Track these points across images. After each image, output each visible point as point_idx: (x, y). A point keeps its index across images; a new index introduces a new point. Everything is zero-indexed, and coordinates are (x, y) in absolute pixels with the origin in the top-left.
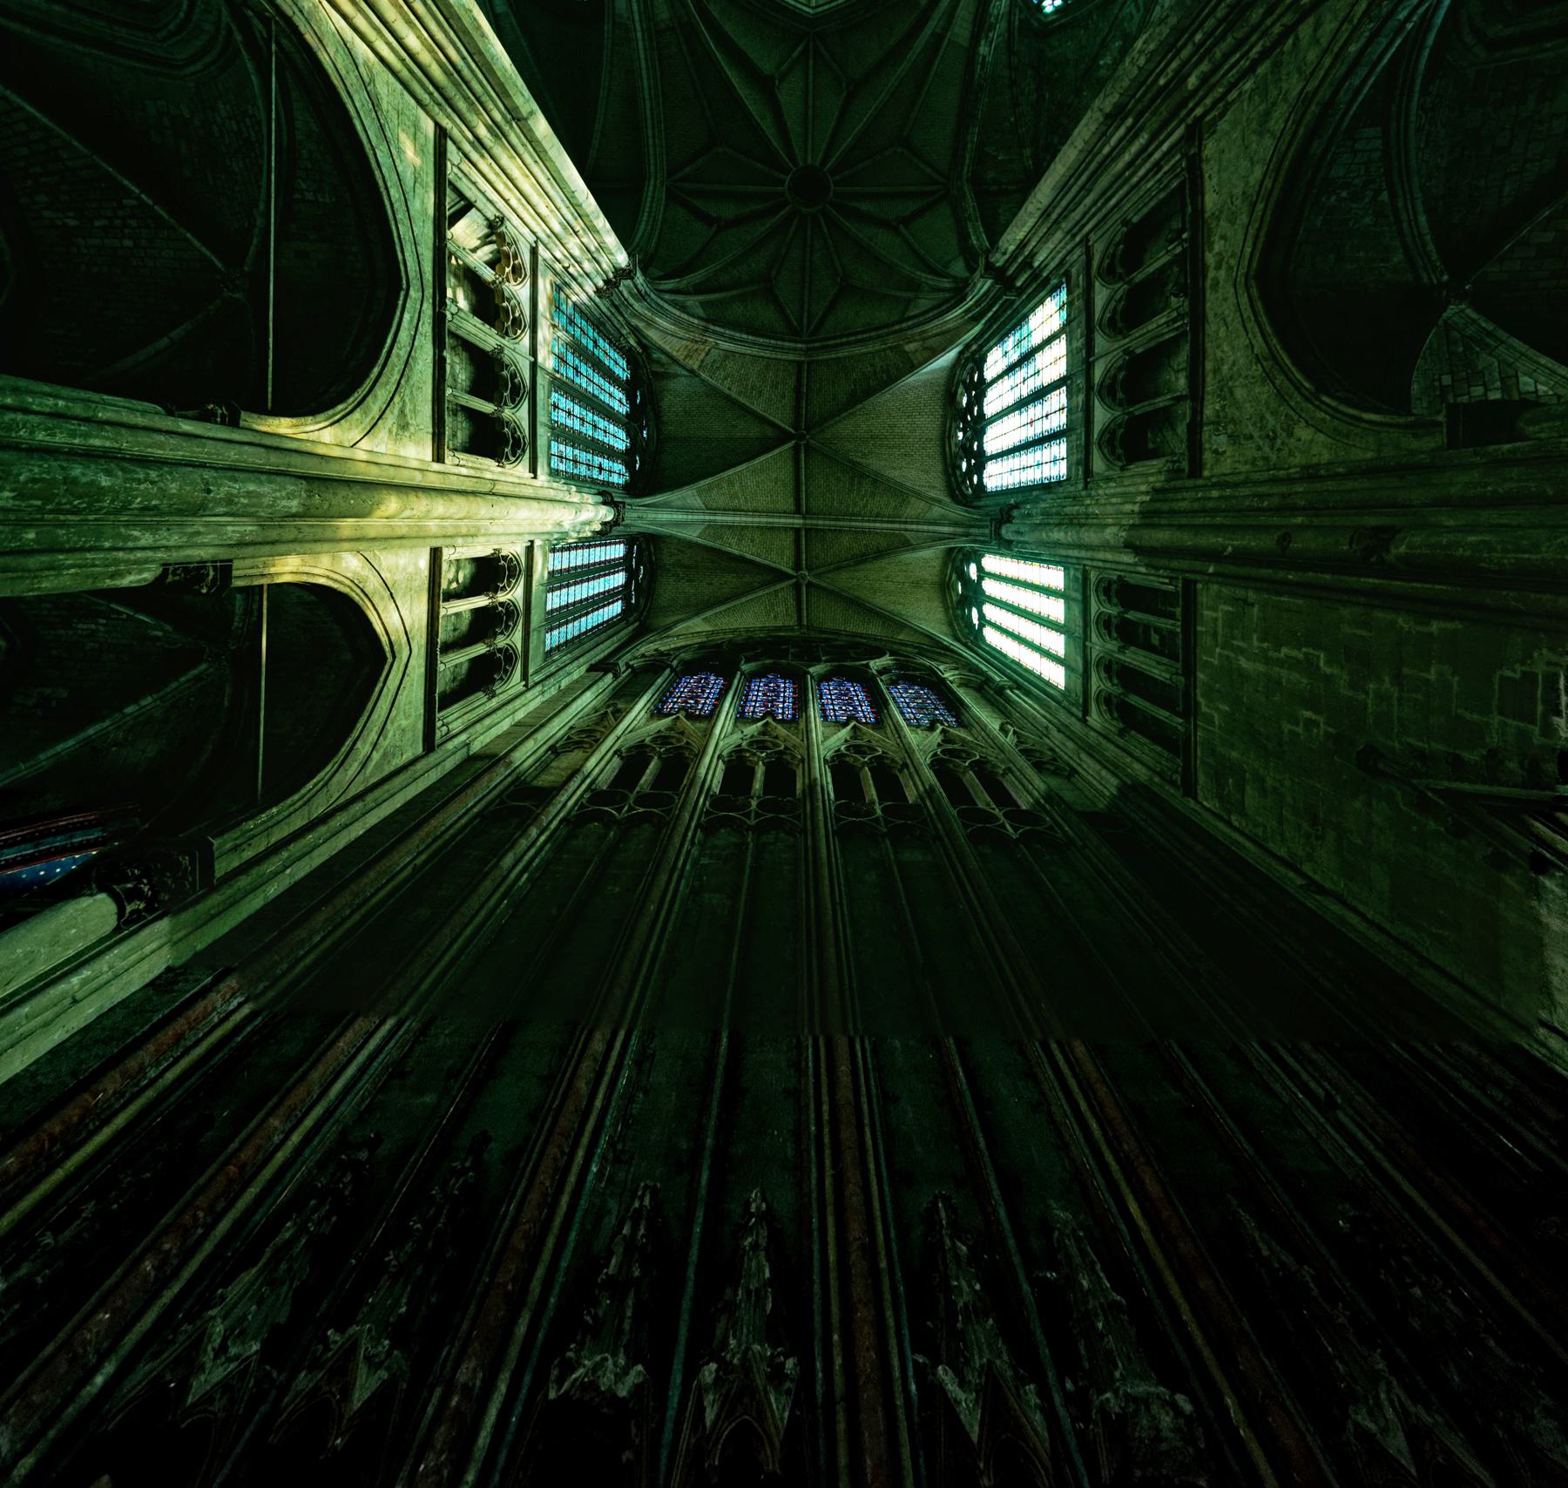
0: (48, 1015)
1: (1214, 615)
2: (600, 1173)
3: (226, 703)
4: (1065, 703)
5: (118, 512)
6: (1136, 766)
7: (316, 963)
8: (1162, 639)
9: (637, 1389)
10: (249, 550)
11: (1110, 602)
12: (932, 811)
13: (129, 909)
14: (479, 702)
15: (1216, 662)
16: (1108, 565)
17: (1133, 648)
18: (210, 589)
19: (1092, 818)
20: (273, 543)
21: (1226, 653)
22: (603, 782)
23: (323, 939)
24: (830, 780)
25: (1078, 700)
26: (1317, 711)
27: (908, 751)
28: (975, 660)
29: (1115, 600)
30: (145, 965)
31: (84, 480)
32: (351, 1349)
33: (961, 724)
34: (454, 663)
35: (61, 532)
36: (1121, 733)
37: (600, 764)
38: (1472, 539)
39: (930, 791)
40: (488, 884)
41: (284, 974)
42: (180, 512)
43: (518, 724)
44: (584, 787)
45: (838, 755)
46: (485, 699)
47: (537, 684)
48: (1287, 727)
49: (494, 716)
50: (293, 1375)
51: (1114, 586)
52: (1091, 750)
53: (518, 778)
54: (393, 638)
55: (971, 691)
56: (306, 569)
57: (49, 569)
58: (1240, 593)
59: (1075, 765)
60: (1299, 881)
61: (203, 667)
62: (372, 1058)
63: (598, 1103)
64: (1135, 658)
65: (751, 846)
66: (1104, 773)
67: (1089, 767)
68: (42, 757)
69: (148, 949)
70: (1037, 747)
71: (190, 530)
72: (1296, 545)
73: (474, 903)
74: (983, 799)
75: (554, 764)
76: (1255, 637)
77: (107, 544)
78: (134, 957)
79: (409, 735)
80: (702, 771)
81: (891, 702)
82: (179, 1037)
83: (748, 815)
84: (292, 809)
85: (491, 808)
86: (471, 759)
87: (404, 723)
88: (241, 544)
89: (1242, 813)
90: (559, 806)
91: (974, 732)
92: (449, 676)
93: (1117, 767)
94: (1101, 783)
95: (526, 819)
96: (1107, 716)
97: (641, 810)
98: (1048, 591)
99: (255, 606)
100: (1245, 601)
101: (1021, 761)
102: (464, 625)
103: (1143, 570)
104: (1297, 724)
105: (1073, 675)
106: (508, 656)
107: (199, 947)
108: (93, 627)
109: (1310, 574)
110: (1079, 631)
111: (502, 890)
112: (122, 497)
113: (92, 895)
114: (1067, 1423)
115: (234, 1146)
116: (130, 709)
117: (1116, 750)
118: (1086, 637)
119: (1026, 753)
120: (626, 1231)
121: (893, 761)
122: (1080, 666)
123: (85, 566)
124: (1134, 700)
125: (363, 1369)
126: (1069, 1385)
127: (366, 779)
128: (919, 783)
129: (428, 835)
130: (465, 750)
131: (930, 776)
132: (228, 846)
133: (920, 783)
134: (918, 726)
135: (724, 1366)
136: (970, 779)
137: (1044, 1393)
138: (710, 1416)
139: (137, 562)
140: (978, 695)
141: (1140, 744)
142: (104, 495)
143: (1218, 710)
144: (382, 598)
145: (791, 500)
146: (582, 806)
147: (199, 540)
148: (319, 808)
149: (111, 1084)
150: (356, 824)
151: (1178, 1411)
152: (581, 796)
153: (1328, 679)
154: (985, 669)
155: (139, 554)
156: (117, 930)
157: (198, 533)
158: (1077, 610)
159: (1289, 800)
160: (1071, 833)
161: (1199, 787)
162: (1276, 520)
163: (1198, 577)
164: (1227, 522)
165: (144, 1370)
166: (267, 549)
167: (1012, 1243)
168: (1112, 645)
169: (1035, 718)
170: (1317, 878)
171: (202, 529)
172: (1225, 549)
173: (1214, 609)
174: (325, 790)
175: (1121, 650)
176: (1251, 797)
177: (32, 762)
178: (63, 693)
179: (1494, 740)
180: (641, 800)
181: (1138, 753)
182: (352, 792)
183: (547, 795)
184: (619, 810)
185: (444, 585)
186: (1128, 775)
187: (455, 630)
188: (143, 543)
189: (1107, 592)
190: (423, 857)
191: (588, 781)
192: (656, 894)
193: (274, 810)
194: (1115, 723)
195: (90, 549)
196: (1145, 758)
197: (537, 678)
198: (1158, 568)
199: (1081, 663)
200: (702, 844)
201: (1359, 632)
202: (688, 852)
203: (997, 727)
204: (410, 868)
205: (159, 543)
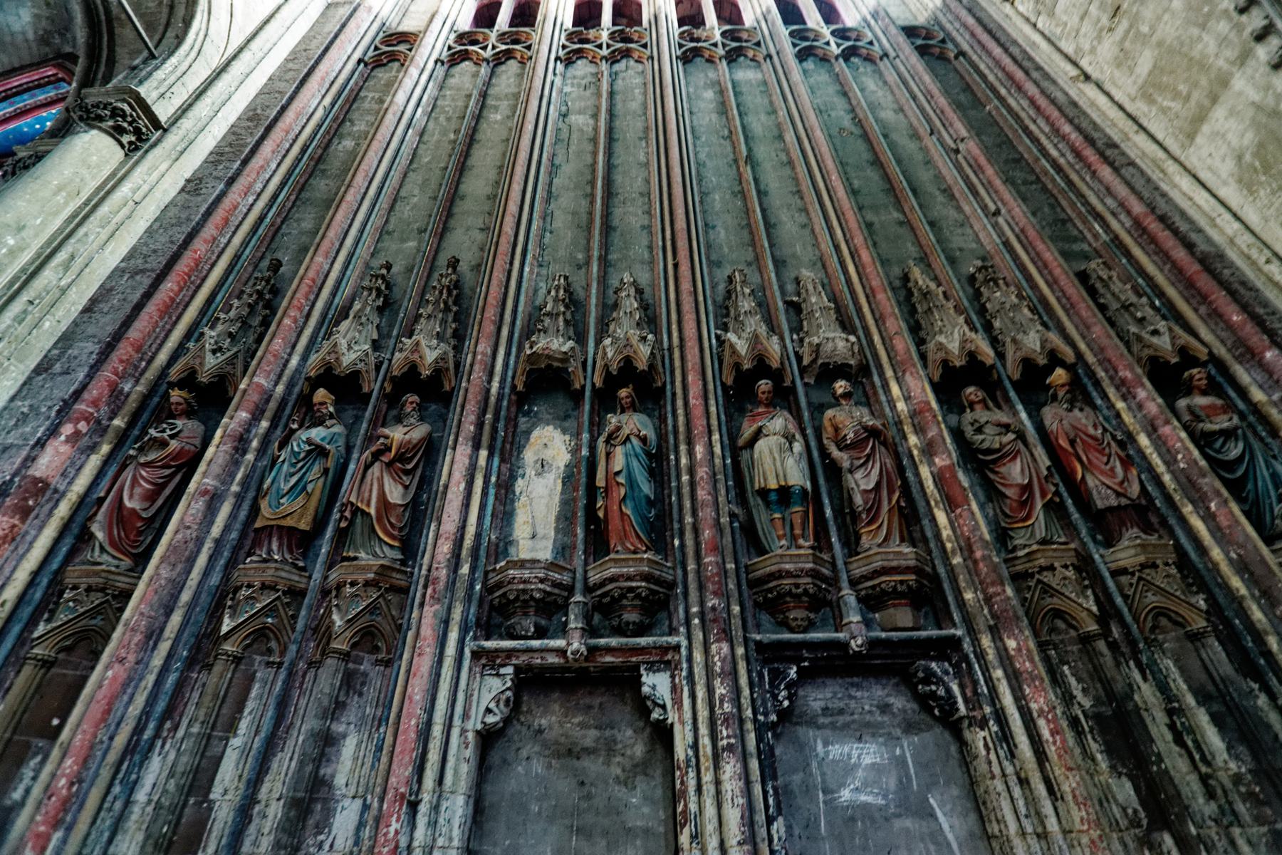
2: (531, 272)
9: (572, 349)
23: (279, 165)
32: (418, 344)
40: (390, 119)
60: (1074, 72)
62: (364, 225)
73: (384, 132)
83: (600, 46)
89: (1051, 14)
120: (553, 293)
125: (427, 351)
129: (323, 79)
146: (450, 48)
167: (776, 287)
180: (502, 37)
184: (484, 48)
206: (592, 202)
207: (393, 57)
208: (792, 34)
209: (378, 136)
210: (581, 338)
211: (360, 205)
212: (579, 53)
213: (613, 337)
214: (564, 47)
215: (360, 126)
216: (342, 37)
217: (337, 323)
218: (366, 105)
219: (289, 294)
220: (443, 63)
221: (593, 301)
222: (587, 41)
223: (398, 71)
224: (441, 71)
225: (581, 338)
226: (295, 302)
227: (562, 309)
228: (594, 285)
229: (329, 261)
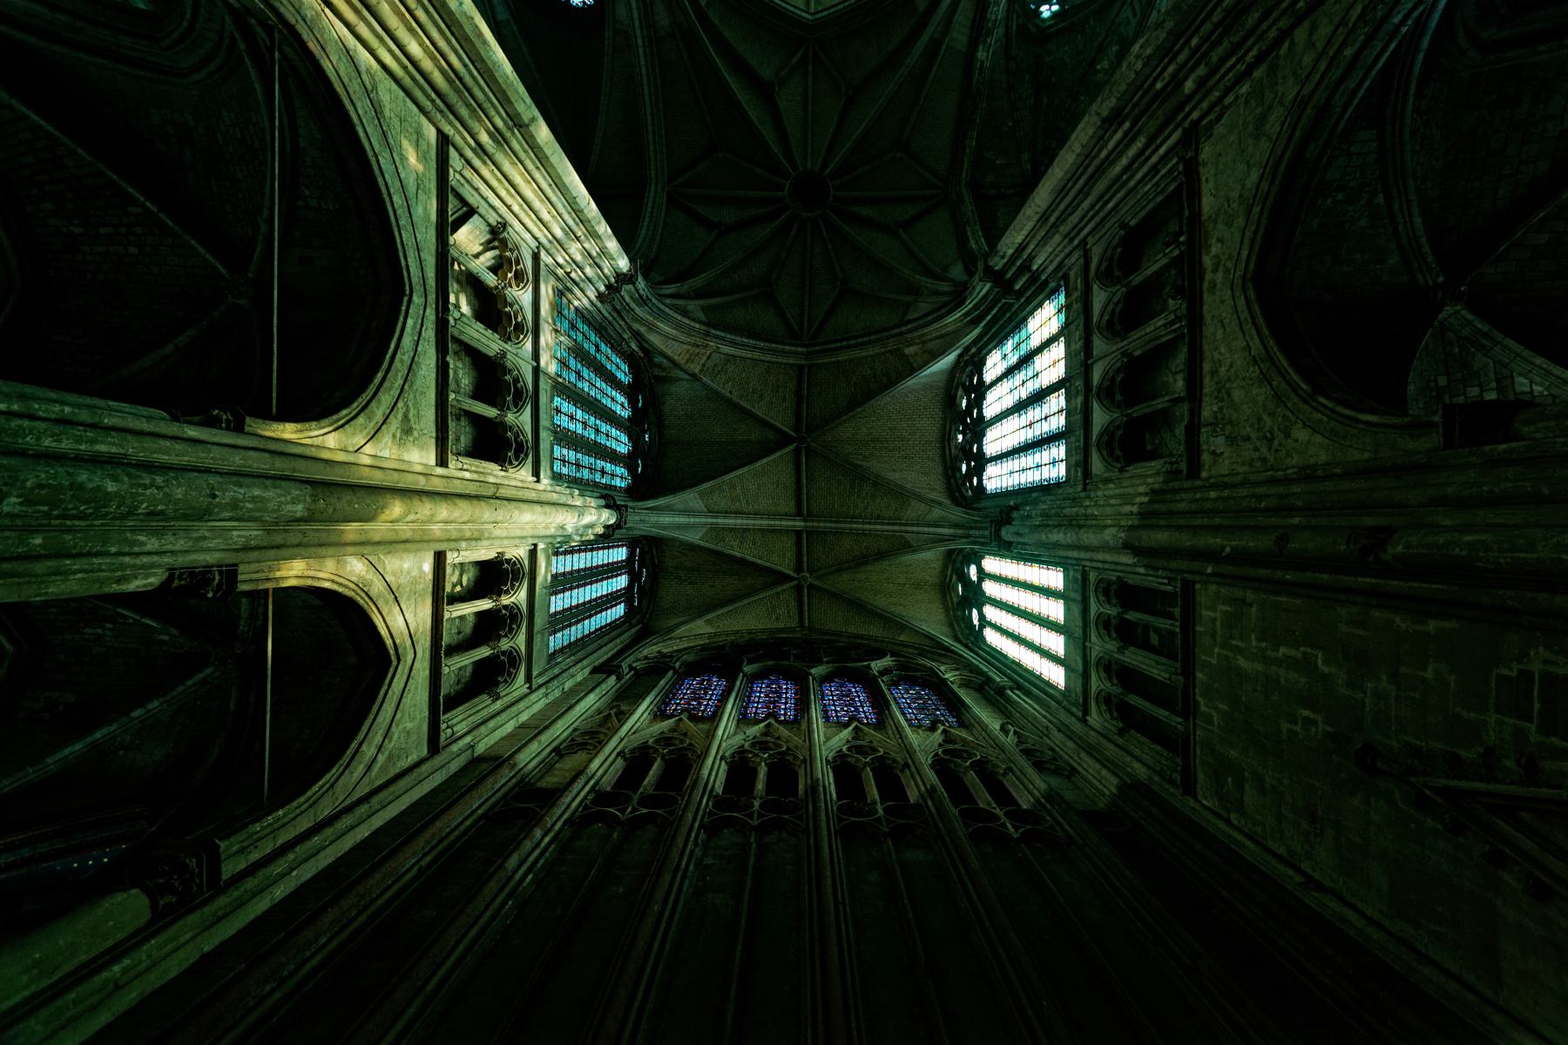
1: (1213, 615)
3: (232, 706)
4: (1065, 703)
5: (123, 517)
6: (1136, 765)
10: (254, 555)
11: (1109, 602)
12: (933, 811)
13: (162, 903)
14: (484, 705)
15: (1214, 662)
16: (1106, 566)
17: (1132, 648)
18: (215, 593)
20: (278, 547)
21: (1225, 652)
23: (330, 940)
24: (832, 780)
25: (1077, 699)
27: (909, 751)
28: (975, 660)
29: (1114, 601)
30: (181, 954)
31: (90, 485)
33: (962, 724)
34: (458, 666)
35: (67, 537)
36: (1121, 733)
37: (603, 766)
38: (1468, 538)
39: (932, 791)
40: (493, 885)
41: (291, 975)
42: (186, 517)
43: (522, 726)
44: (588, 788)
45: (840, 755)
46: (489, 701)
47: (540, 686)
48: (1285, 726)
49: (498, 718)
51: (1114, 587)
52: (1091, 750)
53: (522, 779)
54: (398, 641)
55: (971, 691)
56: (311, 573)
57: (55, 574)
58: (1239, 593)
59: (1075, 764)
60: (1299, 879)
61: (209, 671)
64: (1134, 658)
66: (1104, 772)
67: (1088, 766)
68: (50, 760)
70: (1037, 747)
71: (196, 535)
72: (1294, 546)
74: (984, 799)
75: (557, 766)
76: (1253, 637)
77: (113, 550)
78: (169, 947)
79: (414, 737)
80: (705, 772)
81: (892, 703)
84: (298, 811)
85: (496, 810)
86: (475, 761)
87: (409, 725)
88: (247, 548)
90: (563, 808)
91: (975, 732)
92: (453, 678)
94: (1101, 782)
95: (530, 820)
96: (1107, 716)
97: (644, 811)
98: (1047, 592)
99: (261, 610)
100: (1243, 601)
101: (1022, 761)
102: (468, 629)
103: (1142, 570)
104: (1296, 723)
105: (1072, 675)
106: (512, 659)
107: (207, 949)
108: (100, 631)
109: (1308, 574)
110: (1079, 632)
111: (507, 890)
112: (128, 502)
113: (125, 890)
117: (1117, 750)
119: (1026, 752)
121: (894, 761)
122: (1080, 667)
123: (92, 571)
124: (1134, 699)
127: (371, 782)
128: (920, 783)
130: (469, 752)
131: (931, 776)
132: (235, 848)
133: (921, 782)
134: (920, 727)
136: (971, 778)
139: (142, 567)
140: (978, 695)
141: (1139, 743)
142: (110, 501)
143: (1216, 708)
144: (387, 602)
145: (793, 503)
146: (586, 807)
147: (205, 544)
148: (325, 810)
150: (362, 826)
152: (585, 798)
154: (985, 669)
155: (145, 559)
156: (151, 922)
157: (204, 538)
158: (1076, 610)
160: (1071, 832)
161: (1198, 786)
162: (1274, 521)
163: (1197, 578)
164: (1225, 522)
166: (272, 553)
168: (1112, 646)
169: (1035, 718)
170: (1316, 875)
171: (207, 534)
172: (1223, 549)
173: (1214, 610)
174: (331, 792)
175: (1121, 650)
177: (41, 766)
181: (1137, 752)
185: (448, 589)
186: (1128, 774)
187: (459, 633)
188: (149, 548)
189: (1106, 593)
190: (428, 859)
191: (592, 782)
192: (659, 895)
193: (281, 812)
194: (1114, 722)
195: (96, 555)
197: (541, 681)
198: (1157, 569)
199: (1078, 662)
201: (1356, 631)
203: (998, 727)
204: (416, 869)
205: (165, 548)
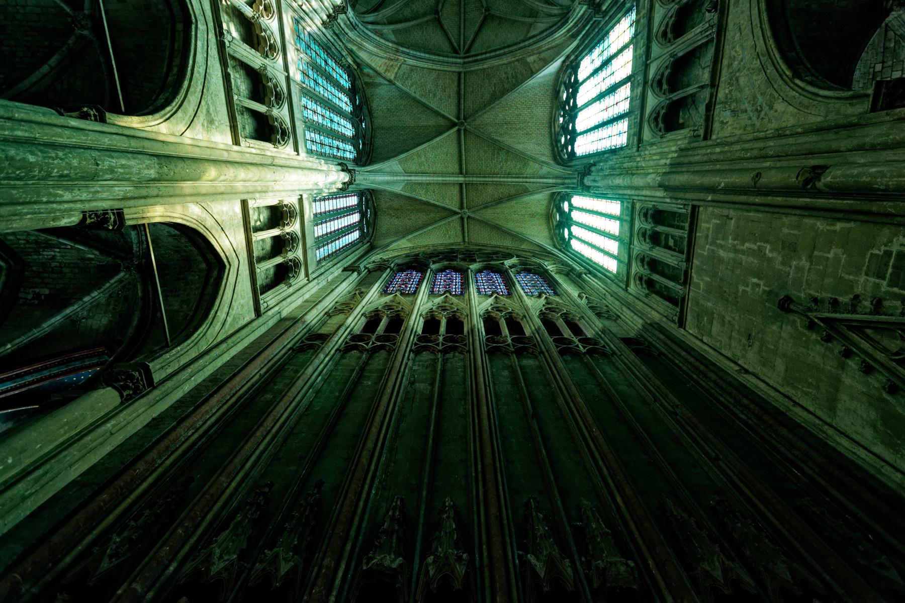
0: (101, 440)
1: (708, 226)
2: (376, 494)
3: (140, 294)
5: (44, 178)
6: (654, 313)
7: (216, 422)
8: (675, 242)
9: (401, 565)
10: (131, 203)
11: (646, 220)
12: (539, 339)
13: (125, 394)
14: (282, 290)
17: (658, 248)
18: (114, 226)
19: (627, 341)
20: (145, 197)
21: (712, 248)
22: (358, 330)
23: (218, 410)
24: (482, 325)
25: (624, 279)
26: (760, 279)
27: (526, 309)
28: (565, 258)
30: (141, 418)
31: (18, 158)
33: (556, 294)
34: (266, 268)
35: (14, 192)
36: (647, 296)
37: (355, 321)
38: (873, 170)
39: (539, 329)
40: (300, 383)
41: (201, 426)
42: (83, 178)
43: (306, 301)
44: (347, 332)
45: (487, 312)
46: (286, 288)
47: (314, 279)
48: (741, 288)
49: (292, 297)
50: (254, 564)
51: (650, 212)
52: (628, 306)
53: (310, 329)
54: (227, 254)
56: (169, 214)
59: (619, 314)
60: (737, 368)
61: (122, 274)
63: (373, 467)
64: (659, 253)
65: (440, 360)
66: (635, 317)
67: (627, 314)
69: (140, 411)
70: (598, 305)
71: (92, 190)
72: (763, 180)
73: (294, 391)
74: (567, 333)
75: (329, 322)
76: (730, 238)
77: (45, 199)
78: (134, 415)
80: (411, 323)
81: (517, 283)
82: (167, 447)
84: (188, 348)
85: (297, 345)
86: (282, 320)
87: (242, 302)
88: (125, 199)
89: (710, 335)
90: (334, 343)
92: (263, 276)
93: (643, 314)
94: (632, 324)
95: (316, 349)
96: (640, 287)
97: (379, 343)
98: (610, 217)
99: (144, 238)
100: (727, 217)
101: (590, 313)
102: (268, 246)
103: (668, 200)
104: (748, 286)
107: (154, 416)
109: (769, 198)
110: (627, 240)
111: (308, 385)
112: (45, 168)
113: (104, 388)
114: (581, 571)
115: (206, 488)
116: (86, 299)
117: (644, 306)
118: (631, 242)
120: (390, 513)
121: (518, 314)
122: (626, 261)
123: (35, 213)
126: (583, 559)
127: (226, 332)
128: (532, 326)
129: (265, 358)
130: (279, 315)
131: (538, 322)
132: (158, 367)
133: (532, 326)
134: (532, 296)
135: (437, 558)
136: (561, 323)
137: (573, 562)
138: (431, 573)
139: (65, 210)
142: (34, 168)
143: (702, 280)
144: (217, 231)
146: (347, 343)
147: (99, 196)
148: (203, 347)
149: (141, 466)
150: (225, 355)
151: (627, 565)
152: (346, 338)
153: (770, 260)
155: (66, 206)
156: (122, 403)
157: (98, 192)
158: (627, 227)
159: (737, 327)
160: (614, 348)
161: (687, 323)
163: (701, 203)
164: (723, 168)
165: (189, 566)
166: (142, 201)
167: (563, 513)
168: (646, 247)
169: (598, 290)
170: (746, 366)
173: (708, 222)
174: (204, 337)
175: (651, 249)
176: (716, 328)
178: (47, 291)
179: (859, 290)
180: (379, 338)
181: (655, 306)
182: (220, 338)
183: (324, 338)
184: (367, 344)
185: (252, 223)
186: (648, 318)
187: (263, 249)
188: (65, 198)
190: (264, 370)
191: (349, 330)
192: (390, 384)
193: (179, 348)
194: (643, 290)
195: (35, 203)
196: (659, 309)
197: (314, 276)
198: (677, 199)
200: (414, 360)
201: (792, 232)
202: (407, 364)
203: (577, 295)
204: (258, 374)
205: (76, 198)
206: (426, 441)
207: (311, 347)
208: (554, 341)
209: (290, 394)
210: (409, 559)
211: (264, 438)
212: (425, 348)
213: (436, 556)
214: (416, 344)
215: (279, 386)
216: (284, 336)
217: (218, 534)
218: (287, 374)
219: (191, 506)
220: (340, 351)
221: (421, 520)
222: (431, 341)
223: (312, 354)
224: (338, 356)
225: (409, 558)
226: (192, 514)
227: (396, 528)
228: (423, 507)
229: (229, 480)
